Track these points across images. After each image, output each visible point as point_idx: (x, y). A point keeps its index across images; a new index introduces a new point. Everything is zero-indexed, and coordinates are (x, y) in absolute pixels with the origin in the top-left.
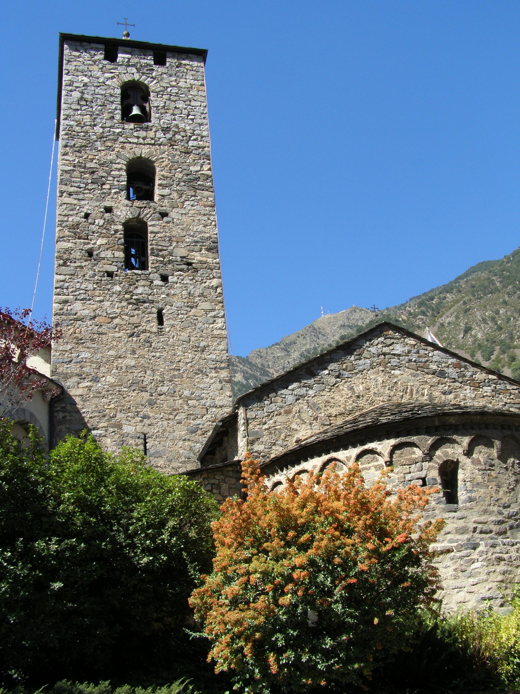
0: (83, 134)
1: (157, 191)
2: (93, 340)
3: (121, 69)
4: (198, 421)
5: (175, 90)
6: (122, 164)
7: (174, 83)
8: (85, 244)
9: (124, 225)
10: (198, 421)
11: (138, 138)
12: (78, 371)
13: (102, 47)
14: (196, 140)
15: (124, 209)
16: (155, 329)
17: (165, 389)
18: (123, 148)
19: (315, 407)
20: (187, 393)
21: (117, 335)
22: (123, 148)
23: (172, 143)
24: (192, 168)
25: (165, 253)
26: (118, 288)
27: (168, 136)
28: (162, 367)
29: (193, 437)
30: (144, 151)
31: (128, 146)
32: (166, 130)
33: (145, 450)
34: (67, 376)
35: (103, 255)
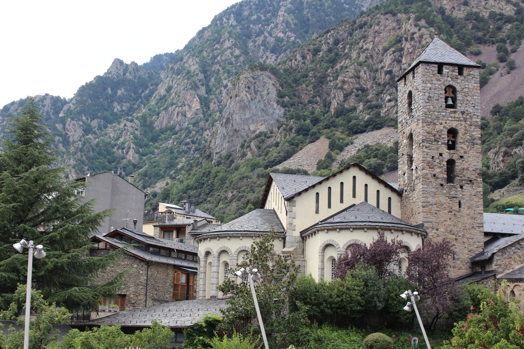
0: (430, 116)
1: (458, 146)
2: (436, 213)
3: (446, 78)
4: (472, 247)
5: (466, 90)
6: (445, 132)
7: (466, 86)
8: (433, 171)
9: (447, 162)
10: (472, 247)
11: (451, 117)
12: (431, 226)
13: (436, 66)
14: (475, 118)
15: (447, 156)
16: (458, 210)
17: (461, 234)
18: (446, 123)
19: (520, 257)
20: (468, 236)
21: (444, 212)
22: (446, 123)
23: (465, 120)
24: (473, 133)
25: (462, 175)
26: (444, 191)
27: (464, 116)
28: (460, 225)
29: (470, 253)
30: (454, 124)
31: (448, 122)
32: (463, 113)
33: (454, 258)
34: (427, 228)
35: (439, 176)
